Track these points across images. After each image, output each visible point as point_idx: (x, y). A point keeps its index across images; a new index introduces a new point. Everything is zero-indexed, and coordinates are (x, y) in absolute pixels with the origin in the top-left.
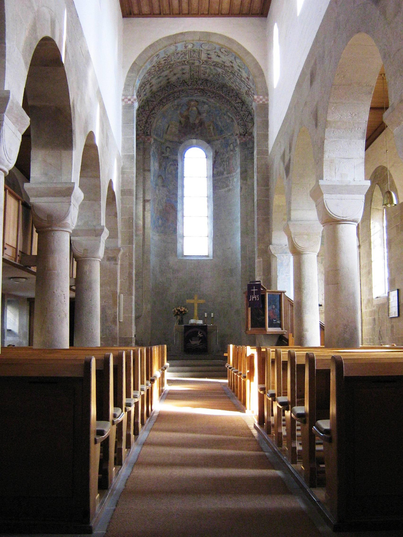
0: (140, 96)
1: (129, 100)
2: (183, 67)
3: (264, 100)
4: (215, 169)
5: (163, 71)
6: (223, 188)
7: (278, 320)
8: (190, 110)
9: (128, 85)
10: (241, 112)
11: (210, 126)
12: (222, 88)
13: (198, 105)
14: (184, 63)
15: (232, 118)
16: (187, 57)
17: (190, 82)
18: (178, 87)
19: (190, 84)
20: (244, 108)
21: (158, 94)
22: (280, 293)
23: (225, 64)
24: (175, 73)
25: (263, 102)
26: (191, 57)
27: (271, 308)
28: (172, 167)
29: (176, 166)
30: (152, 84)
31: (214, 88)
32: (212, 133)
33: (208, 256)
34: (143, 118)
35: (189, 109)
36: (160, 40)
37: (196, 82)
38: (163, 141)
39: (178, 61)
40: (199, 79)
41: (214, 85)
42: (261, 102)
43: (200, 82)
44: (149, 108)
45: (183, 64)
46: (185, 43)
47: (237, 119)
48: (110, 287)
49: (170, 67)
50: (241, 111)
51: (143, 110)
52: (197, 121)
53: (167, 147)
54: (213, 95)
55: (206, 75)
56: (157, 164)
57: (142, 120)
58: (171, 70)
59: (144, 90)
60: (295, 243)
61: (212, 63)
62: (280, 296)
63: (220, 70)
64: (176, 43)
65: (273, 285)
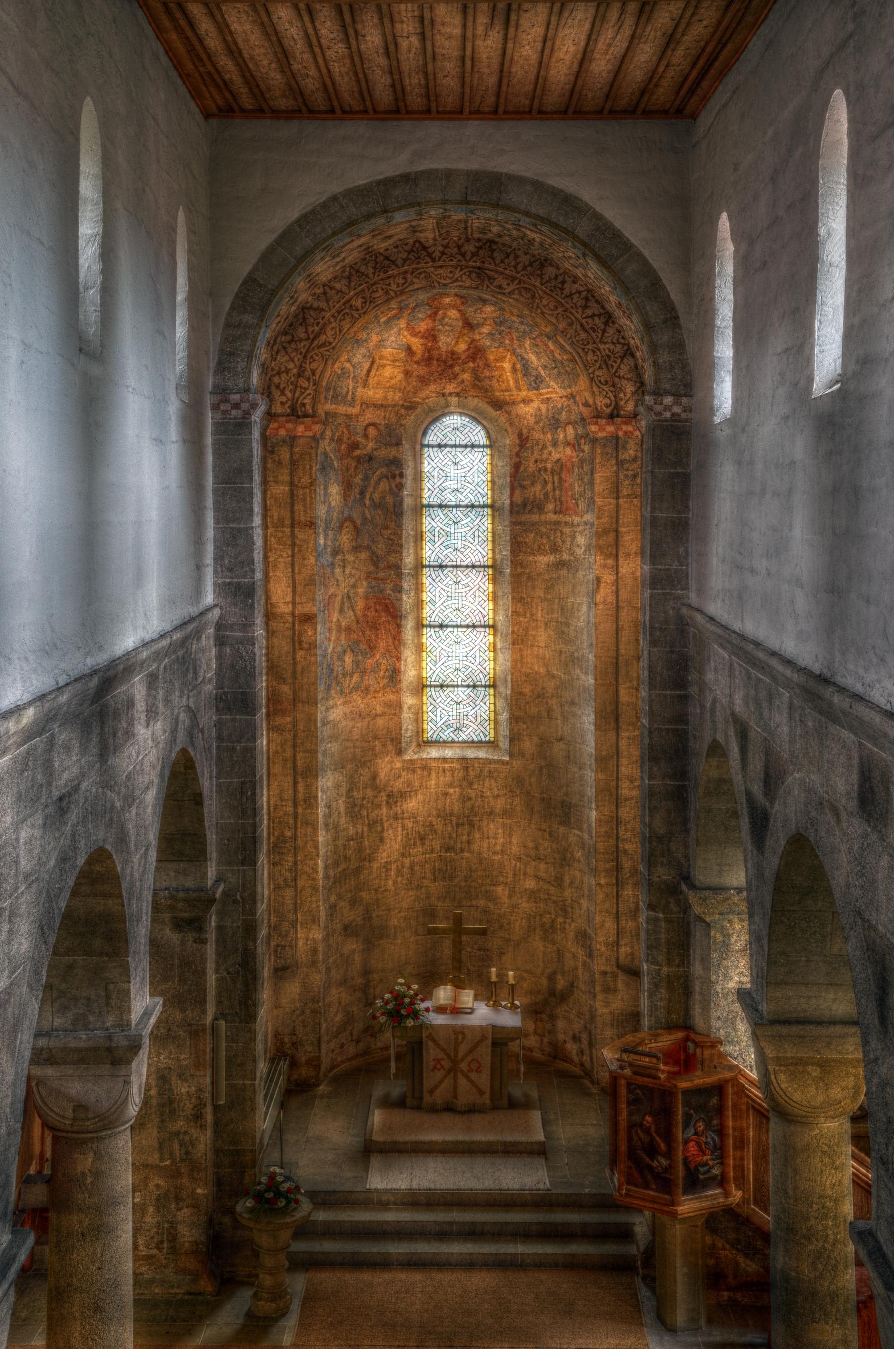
1: (236, 406)
3: (677, 409)
4: (517, 492)
8: (438, 317)
9: (232, 354)
11: (502, 359)
12: (542, 266)
17: (441, 249)
18: (399, 262)
19: (437, 254)
20: (611, 331)
21: (338, 286)
25: (673, 414)
29: (398, 479)
31: (515, 267)
32: (508, 381)
33: (492, 744)
34: (291, 366)
35: (435, 313)
36: (335, 198)
37: (459, 247)
38: (355, 410)
42: (668, 415)
43: (470, 248)
44: (307, 331)
50: (601, 342)
51: (288, 338)
52: (462, 346)
54: (512, 287)
57: (287, 371)
60: (778, 1089)
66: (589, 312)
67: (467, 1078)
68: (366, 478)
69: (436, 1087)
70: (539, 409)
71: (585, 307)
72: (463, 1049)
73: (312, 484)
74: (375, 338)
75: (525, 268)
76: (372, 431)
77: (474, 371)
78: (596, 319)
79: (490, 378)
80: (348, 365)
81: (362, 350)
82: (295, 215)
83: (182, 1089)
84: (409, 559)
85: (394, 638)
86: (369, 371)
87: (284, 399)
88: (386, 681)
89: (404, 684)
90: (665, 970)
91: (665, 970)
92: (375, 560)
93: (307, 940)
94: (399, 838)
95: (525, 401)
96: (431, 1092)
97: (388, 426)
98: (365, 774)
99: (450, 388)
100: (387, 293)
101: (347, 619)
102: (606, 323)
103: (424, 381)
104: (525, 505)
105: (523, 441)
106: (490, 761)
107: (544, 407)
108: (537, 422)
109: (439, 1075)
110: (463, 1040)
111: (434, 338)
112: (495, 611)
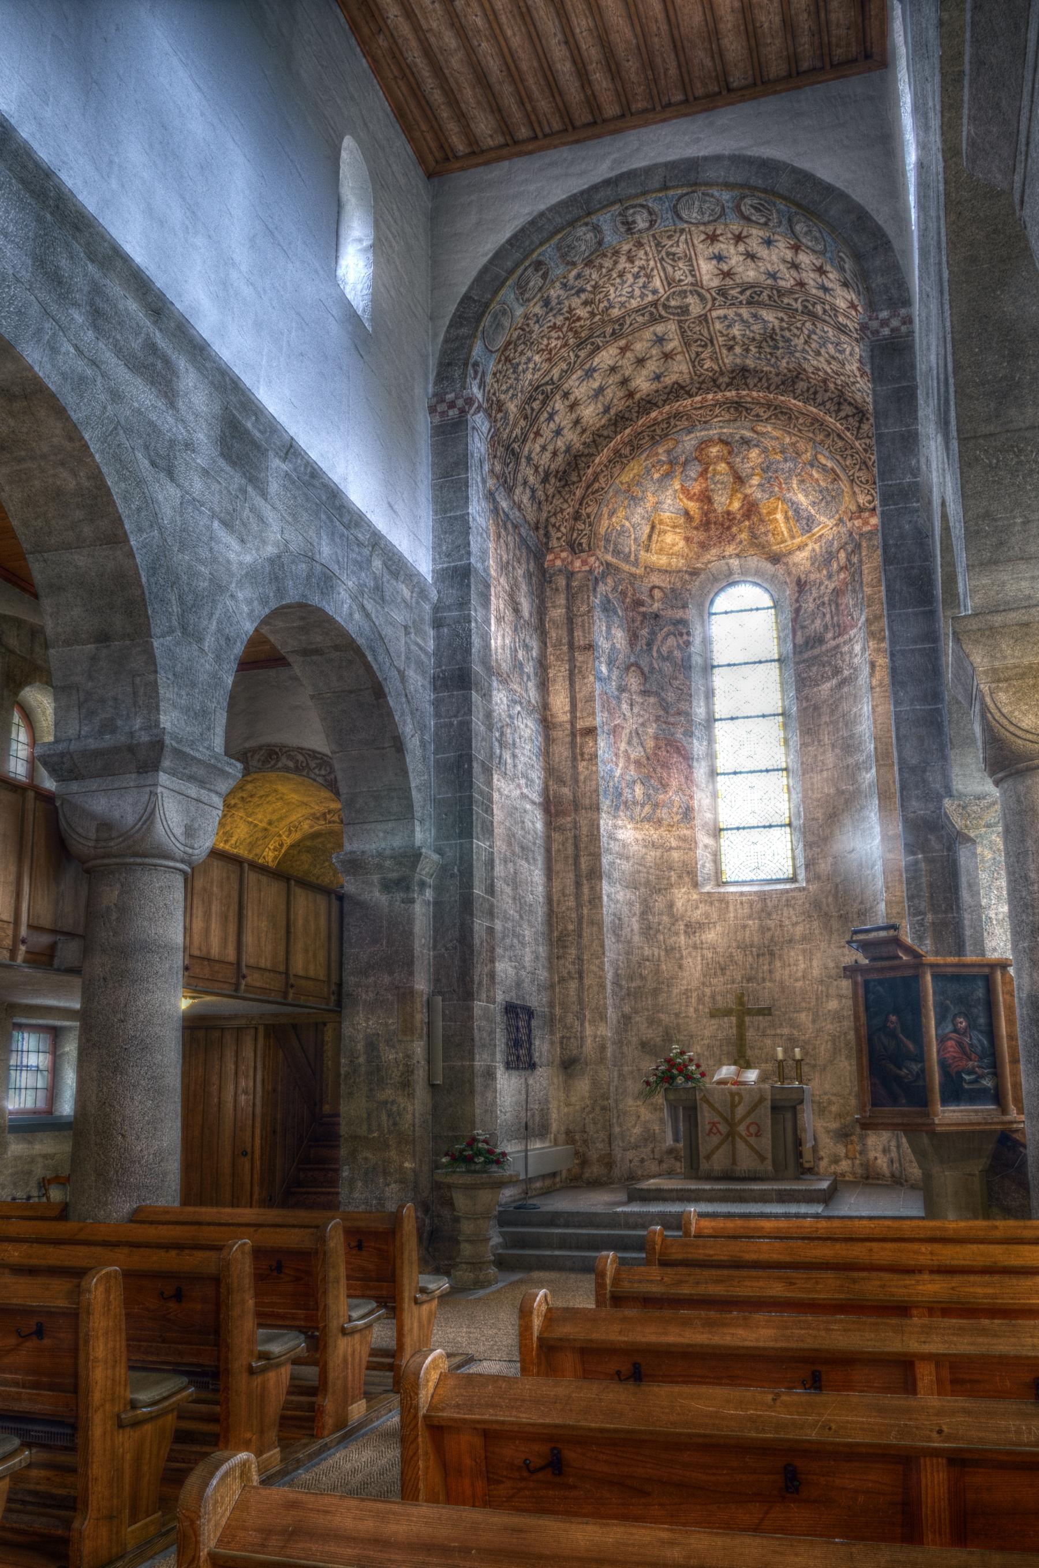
0: (538, 434)
2: (660, 329)
4: (799, 633)
5: (598, 348)
6: (825, 678)
7: (982, 1077)
10: (857, 444)
11: (774, 511)
12: (794, 383)
13: (730, 453)
14: (653, 309)
15: (833, 469)
16: (657, 283)
18: (660, 403)
21: (605, 433)
22: (987, 970)
23: (782, 283)
24: (640, 356)
26: (669, 284)
27: (950, 1028)
28: (671, 641)
29: (685, 637)
30: (572, 398)
31: (768, 388)
35: (706, 470)
37: (714, 381)
38: (639, 571)
39: (634, 303)
40: (722, 373)
41: (768, 380)
45: (655, 319)
46: (617, 208)
47: (844, 469)
48: (391, 973)
49: (614, 333)
52: (736, 505)
53: (654, 587)
54: (769, 414)
55: (738, 350)
56: (619, 636)
58: (622, 343)
59: (545, 415)
61: (742, 293)
62: (988, 982)
63: (769, 316)
64: (589, 214)
65: (969, 947)
66: (842, 414)
67: (746, 1142)
68: (653, 633)
69: (713, 1152)
70: (814, 550)
71: (839, 410)
72: (740, 1111)
73: (589, 611)
74: (651, 499)
75: (777, 387)
76: (657, 594)
77: (751, 529)
78: (851, 419)
79: (765, 534)
80: (627, 524)
81: (640, 510)
82: (508, 235)
83: (390, 1055)
84: (699, 711)
85: (687, 778)
86: (650, 536)
87: (559, 535)
88: (679, 817)
89: (697, 822)
90: (929, 917)
91: (929, 917)
92: (664, 705)
93: (595, 1037)
94: (699, 967)
95: (800, 548)
96: (708, 1157)
97: (673, 590)
98: (659, 903)
99: (730, 550)
100: (653, 438)
101: (636, 753)
102: (861, 422)
103: (704, 546)
104: (807, 643)
105: (801, 585)
106: (787, 891)
107: (817, 547)
108: (812, 564)
109: (716, 1139)
110: (740, 1103)
111: (709, 500)
112: (787, 755)
